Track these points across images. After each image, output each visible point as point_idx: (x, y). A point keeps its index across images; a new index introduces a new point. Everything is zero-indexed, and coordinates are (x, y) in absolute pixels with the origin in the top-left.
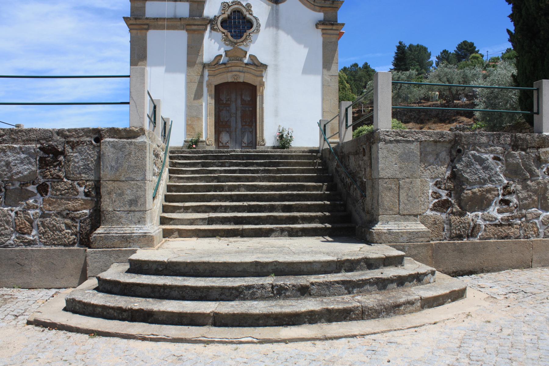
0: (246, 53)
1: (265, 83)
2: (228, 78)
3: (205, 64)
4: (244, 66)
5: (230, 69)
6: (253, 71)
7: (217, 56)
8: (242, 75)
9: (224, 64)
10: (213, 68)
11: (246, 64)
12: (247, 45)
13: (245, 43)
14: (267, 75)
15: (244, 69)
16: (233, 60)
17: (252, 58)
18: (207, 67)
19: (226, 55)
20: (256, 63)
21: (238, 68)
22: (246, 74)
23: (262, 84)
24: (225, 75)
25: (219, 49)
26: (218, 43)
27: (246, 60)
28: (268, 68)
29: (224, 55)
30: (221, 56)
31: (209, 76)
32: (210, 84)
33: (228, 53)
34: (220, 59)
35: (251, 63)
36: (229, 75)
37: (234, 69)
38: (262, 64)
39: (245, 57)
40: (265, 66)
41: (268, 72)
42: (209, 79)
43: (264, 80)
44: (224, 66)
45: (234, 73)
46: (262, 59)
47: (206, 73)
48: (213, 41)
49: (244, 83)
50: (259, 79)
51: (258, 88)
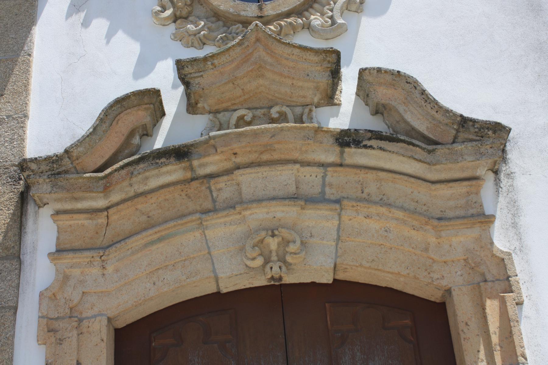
0: (333, 64)
1: (520, 268)
2: (216, 258)
3: (23, 165)
4: (331, 155)
5: (224, 189)
6: (399, 189)
7: (121, 104)
8: (319, 221)
9: (179, 153)
10: (89, 188)
11: (346, 139)
12: (334, 28)
13: (316, 20)
14: (514, 207)
15: (335, 177)
16: (241, 122)
17: (383, 94)
18: (42, 188)
19: (192, 105)
20: (422, 126)
21: (283, 178)
22: (354, 218)
23: (496, 279)
24: (189, 240)
25: (143, 66)
26: (133, 35)
27: (346, 112)
28: (512, 155)
29: (173, 99)
30: (151, 98)
31: (61, 251)
32: (76, 317)
33: (204, 80)
34: (147, 133)
35: (377, 124)
36: (222, 231)
37: (250, 181)
38: (464, 122)
39: (330, 98)
40: (490, 137)
41: (520, 181)
42: (64, 279)
43: (501, 241)
44: (173, 172)
45: (258, 215)
46: (463, 92)
47: (43, 232)
48: (100, 25)
49: (343, 292)
50: (461, 239)
51: (462, 310)
